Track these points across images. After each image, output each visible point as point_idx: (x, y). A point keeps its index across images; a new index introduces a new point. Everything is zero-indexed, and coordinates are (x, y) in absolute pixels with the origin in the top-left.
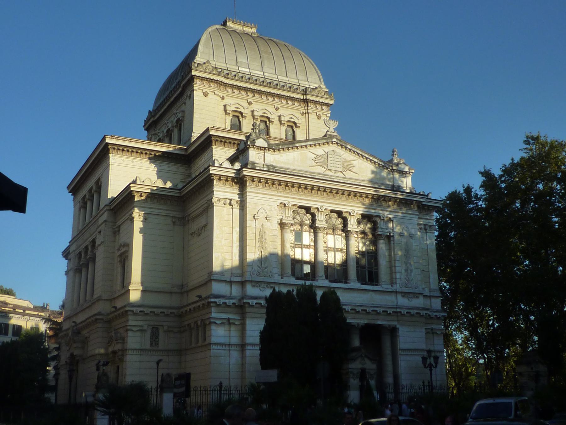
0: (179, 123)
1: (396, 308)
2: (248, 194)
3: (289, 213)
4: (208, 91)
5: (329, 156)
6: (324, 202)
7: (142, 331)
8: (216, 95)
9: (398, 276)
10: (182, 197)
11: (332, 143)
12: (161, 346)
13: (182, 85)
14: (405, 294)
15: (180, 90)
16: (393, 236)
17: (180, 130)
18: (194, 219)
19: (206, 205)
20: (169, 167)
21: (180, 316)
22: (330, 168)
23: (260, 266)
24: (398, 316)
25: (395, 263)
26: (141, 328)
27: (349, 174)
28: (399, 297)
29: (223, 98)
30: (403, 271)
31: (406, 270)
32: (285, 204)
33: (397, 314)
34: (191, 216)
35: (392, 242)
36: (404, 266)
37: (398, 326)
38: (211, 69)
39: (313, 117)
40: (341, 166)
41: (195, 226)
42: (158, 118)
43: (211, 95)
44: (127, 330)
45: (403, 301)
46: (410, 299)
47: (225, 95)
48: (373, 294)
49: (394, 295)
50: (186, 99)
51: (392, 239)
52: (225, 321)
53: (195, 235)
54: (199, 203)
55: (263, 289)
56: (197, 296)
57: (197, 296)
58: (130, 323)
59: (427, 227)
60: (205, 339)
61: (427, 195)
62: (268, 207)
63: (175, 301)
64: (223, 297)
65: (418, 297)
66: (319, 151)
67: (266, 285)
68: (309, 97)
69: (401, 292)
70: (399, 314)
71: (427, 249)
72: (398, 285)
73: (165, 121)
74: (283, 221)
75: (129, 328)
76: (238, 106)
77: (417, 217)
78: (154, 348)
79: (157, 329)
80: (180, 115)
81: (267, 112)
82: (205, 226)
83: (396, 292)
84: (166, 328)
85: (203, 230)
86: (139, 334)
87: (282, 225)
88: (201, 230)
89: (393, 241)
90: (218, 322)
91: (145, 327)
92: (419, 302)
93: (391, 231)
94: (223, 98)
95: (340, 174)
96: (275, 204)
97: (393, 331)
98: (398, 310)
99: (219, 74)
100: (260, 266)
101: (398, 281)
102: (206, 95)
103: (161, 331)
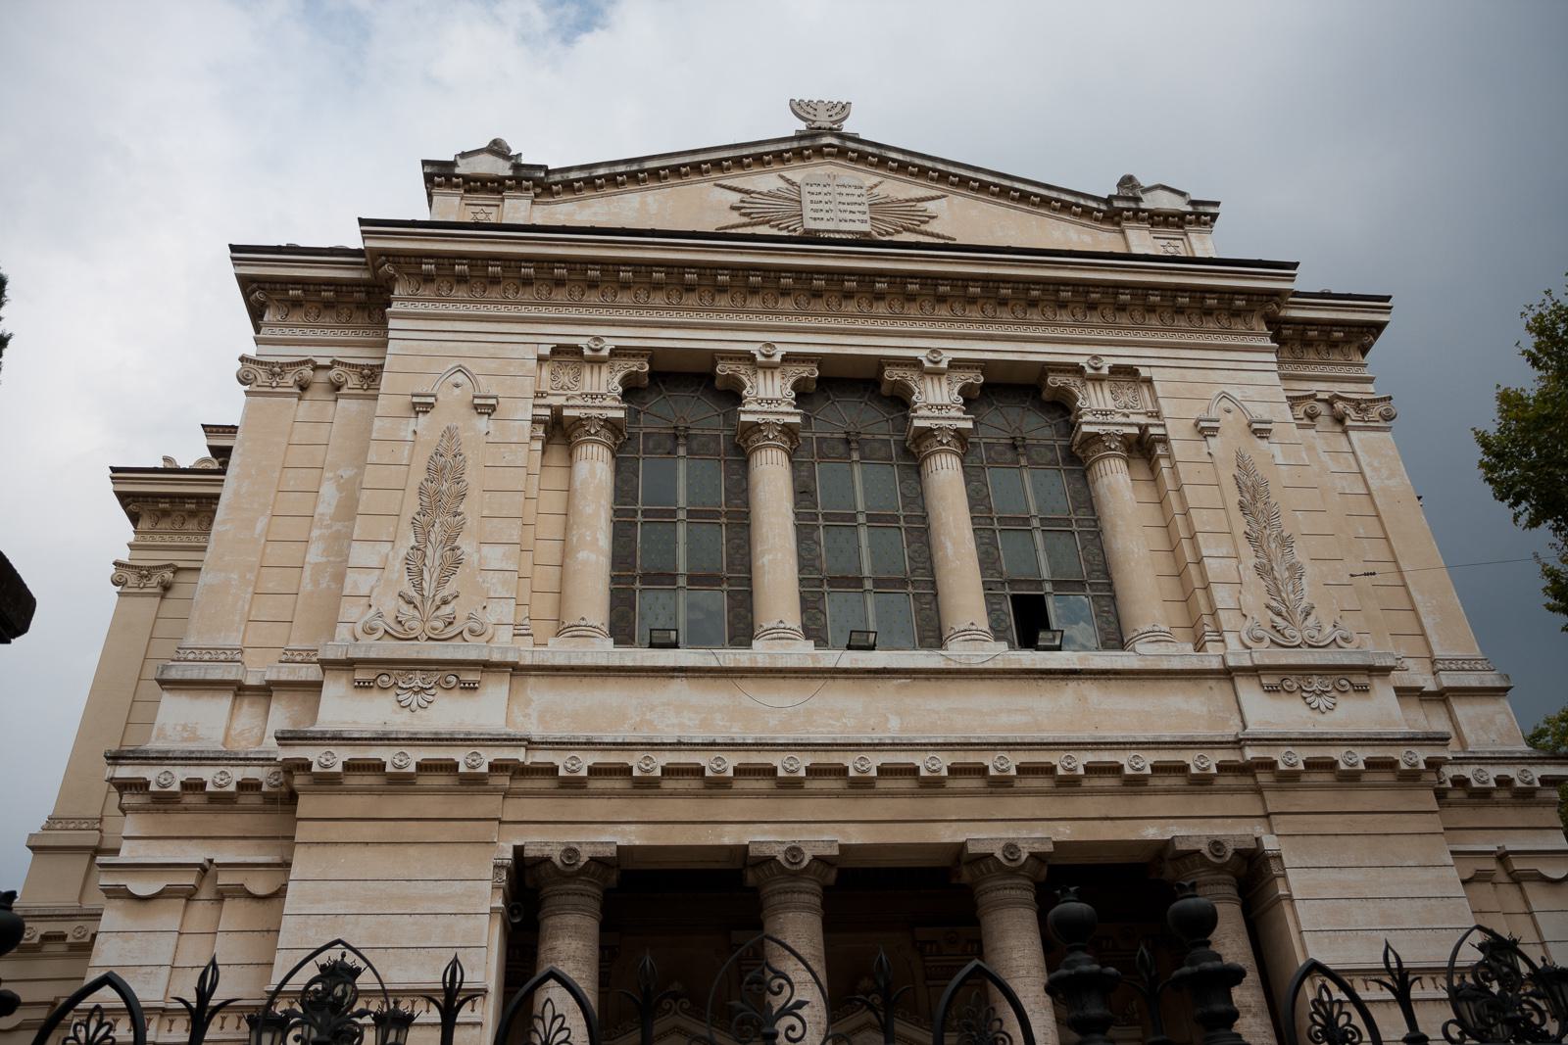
1: (1238, 744)
2: (392, 323)
5: (805, 189)
9: (1222, 596)
14: (1279, 678)
16: (1164, 440)
23: (412, 593)
24: (1258, 791)
25: (1196, 548)
28: (1250, 693)
30: (1250, 576)
31: (1262, 571)
33: (1249, 771)
35: (1164, 463)
36: (1247, 551)
37: (1270, 844)
40: (866, 217)
45: (1268, 713)
46: (1322, 702)
48: (1090, 690)
49: (1219, 691)
51: (1159, 450)
55: (415, 700)
59: (1339, 405)
62: (492, 365)
65: (1363, 690)
67: (436, 677)
69: (1255, 671)
70: (1264, 778)
71: (1369, 494)
72: (1230, 638)
83: (1228, 674)
87: (560, 431)
89: (1169, 457)
92: (1376, 712)
96: (531, 353)
97: (1252, 876)
98: (1251, 753)
100: (412, 593)
101: (1227, 619)
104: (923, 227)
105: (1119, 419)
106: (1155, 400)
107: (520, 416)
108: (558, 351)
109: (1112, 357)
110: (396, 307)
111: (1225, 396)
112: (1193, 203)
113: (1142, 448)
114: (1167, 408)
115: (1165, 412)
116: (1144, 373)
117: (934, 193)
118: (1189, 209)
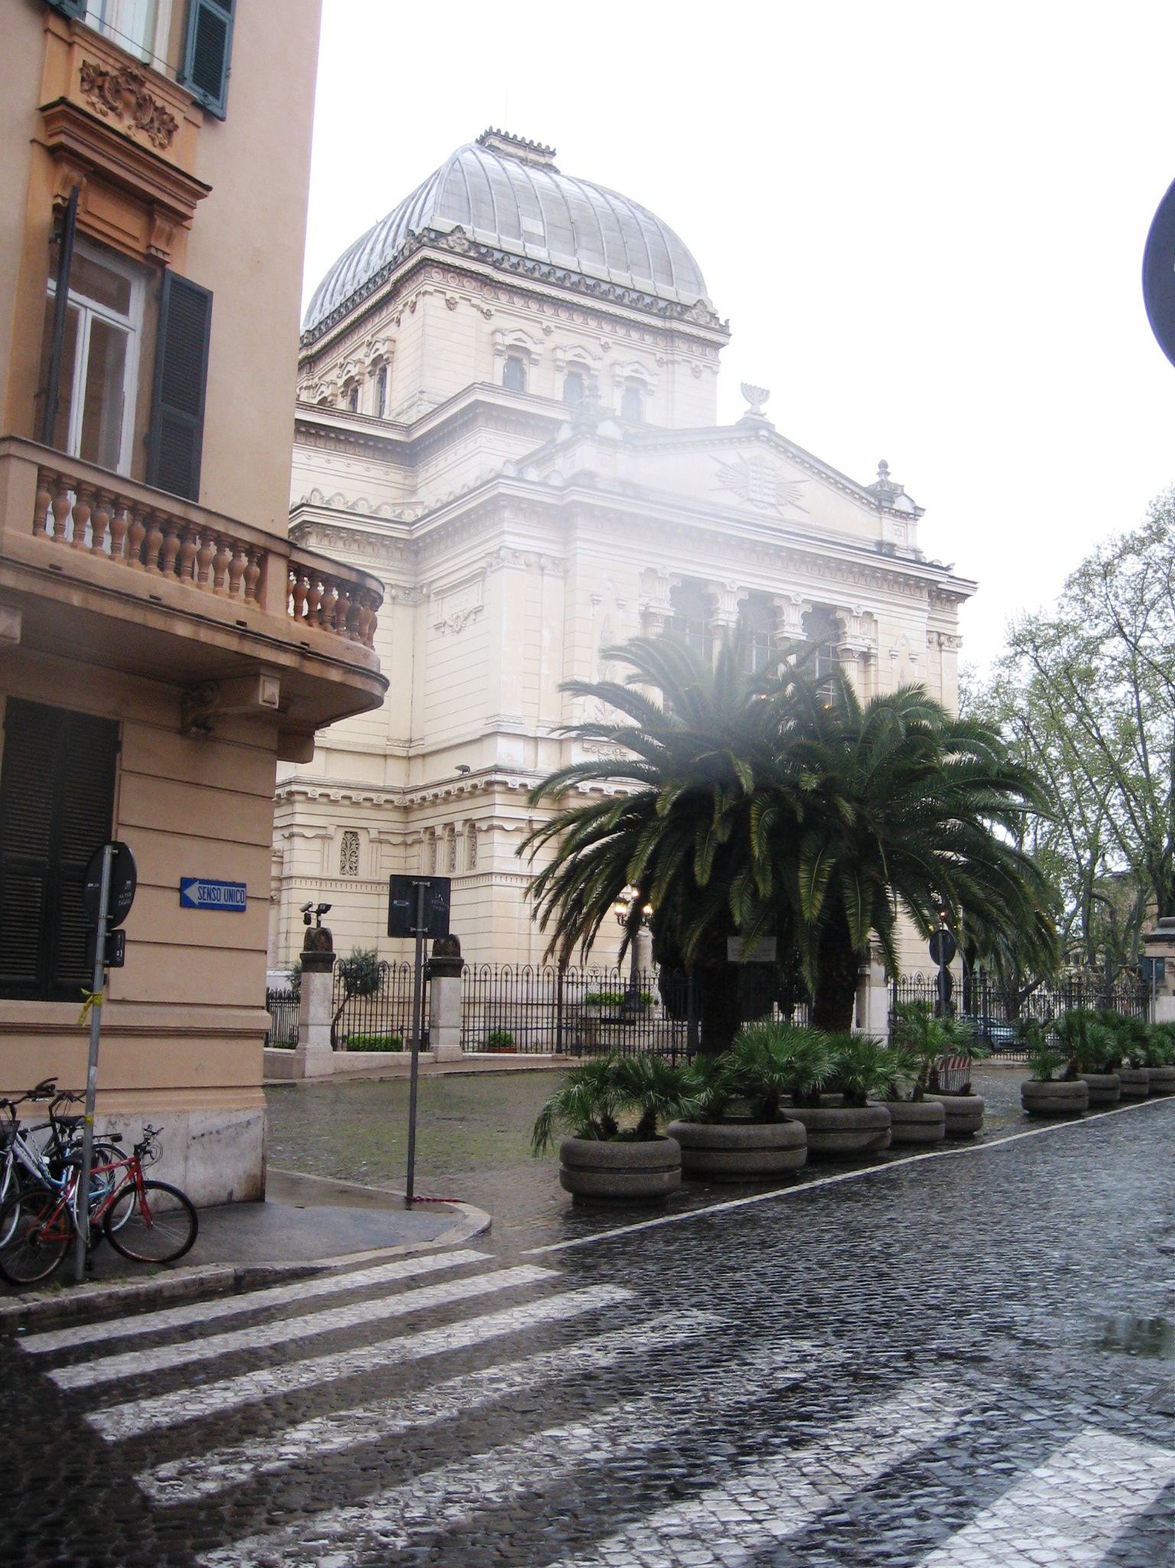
0: (380, 367)
3: (664, 592)
4: (457, 296)
6: (738, 572)
7: (325, 838)
8: (473, 306)
10: (415, 541)
11: (758, 437)
12: (363, 874)
13: (394, 277)
15: (387, 288)
17: (382, 382)
18: (442, 593)
19: (483, 564)
20: (387, 473)
21: (406, 810)
22: (753, 496)
26: (322, 832)
27: (791, 514)
29: (488, 315)
32: (653, 570)
34: (434, 586)
35: (873, 668)
38: (466, 247)
39: (682, 372)
41: (446, 609)
42: (319, 352)
43: (463, 307)
44: (292, 836)
47: (492, 308)
50: (401, 312)
51: (872, 661)
52: (523, 825)
53: (447, 630)
54: (457, 561)
56: (458, 768)
57: (458, 768)
58: (299, 819)
59: (943, 638)
60: (473, 864)
61: (947, 569)
63: (394, 776)
64: (522, 773)
66: (730, 456)
68: (676, 325)
73: (337, 356)
74: (651, 610)
75: (295, 830)
76: (519, 335)
77: (926, 615)
78: (346, 877)
79: (355, 834)
80: (382, 349)
81: (584, 354)
82: (478, 610)
84: (374, 834)
85: (470, 621)
86: (317, 844)
88: (466, 619)
90: (509, 826)
91: (331, 831)
93: (873, 645)
94: (488, 315)
95: (771, 512)
99: (481, 259)
102: (451, 305)
103: (363, 838)
104: (798, 503)
105: (860, 642)
106: (877, 632)
107: (635, 609)
108: (650, 569)
109: (869, 606)
110: (580, 534)
111: (904, 636)
112: (916, 508)
113: (866, 657)
114: (881, 638)
115: (880, 641)
116: (876, 617)
117: (806, 478)
118: (911, 511)
